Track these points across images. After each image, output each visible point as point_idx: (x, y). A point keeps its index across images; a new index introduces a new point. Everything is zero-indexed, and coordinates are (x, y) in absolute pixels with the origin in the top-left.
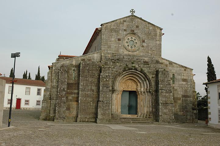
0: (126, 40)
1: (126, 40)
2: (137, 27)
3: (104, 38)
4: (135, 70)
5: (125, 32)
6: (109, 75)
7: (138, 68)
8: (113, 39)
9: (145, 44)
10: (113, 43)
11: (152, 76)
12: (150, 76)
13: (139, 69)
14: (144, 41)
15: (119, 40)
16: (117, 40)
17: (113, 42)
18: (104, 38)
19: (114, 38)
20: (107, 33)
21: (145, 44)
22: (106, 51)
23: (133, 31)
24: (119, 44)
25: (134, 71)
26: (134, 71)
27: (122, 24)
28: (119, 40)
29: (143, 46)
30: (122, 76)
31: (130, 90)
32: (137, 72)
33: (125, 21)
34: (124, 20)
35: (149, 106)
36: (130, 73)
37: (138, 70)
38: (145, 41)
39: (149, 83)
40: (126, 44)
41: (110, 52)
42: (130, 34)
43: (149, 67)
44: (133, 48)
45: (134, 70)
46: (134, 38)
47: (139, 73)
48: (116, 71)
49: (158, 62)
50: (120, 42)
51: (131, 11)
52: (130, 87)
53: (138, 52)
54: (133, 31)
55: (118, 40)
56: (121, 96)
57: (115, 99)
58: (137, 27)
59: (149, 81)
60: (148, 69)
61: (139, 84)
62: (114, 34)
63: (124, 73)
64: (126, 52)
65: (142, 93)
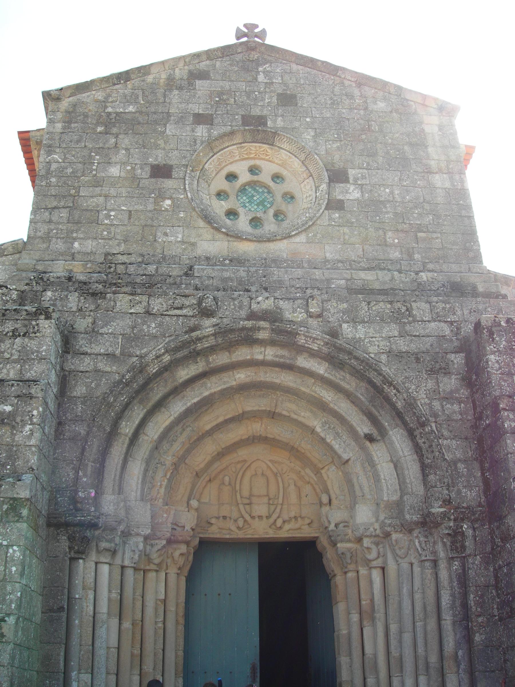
0: (220, 183)
1: (220, 183)
2: (287, 99)
3: (54, 166)
4: (283, 345)
5: (201, 131)
6: (28, 375)
7: (302, 324)
8: (114, 171)
9: (352, 194)
10: (113, 192)
11: (431, 384)
12: (421, 391)
13: (314, 335)
14: (338, 176)
15: (161, 171)
16: (144, 173)
17: (113, 185)
18: (54, 166)
19: (124, 164)
20: (78, 141)
21: (352, 194)
22: (59, 245)
23: (261, 121)
24: (161, 196)
25: (270, 353)
26: (270, 353)
27: (180, 88)
28: (161, 171)
29: (335, 205)
30: (178, 407)
31: (261, 530)
32: (302, 362)
33: (203, 75)
34: (197, 69)
35: (433, 659)
36: (241, 376)
37: (301, 340)
38: (352, 173)
39: (417, 449)
40: (219, 207)
41: (90, 245)
42: (238, 138)
43: (397, 317)
44: (270, 226)
45: (272, 343)
46: (268, 168)
47: (321, 368)
48: (110, 356)
49: (458, 290)
50: (169, 183)
51: (239, 35)
52: (261, 509)
53: (302, 238)
54: (261, 121)
55: (152, 176)
56: (177, 586)
57: (103, 608)
58: (287, 99)
59: (411, 434)
60: (393, 330)
61: (332, 476)
62: (125, 141)
63: (184, 374)
64: (211, 245)
65: (366, 542)
